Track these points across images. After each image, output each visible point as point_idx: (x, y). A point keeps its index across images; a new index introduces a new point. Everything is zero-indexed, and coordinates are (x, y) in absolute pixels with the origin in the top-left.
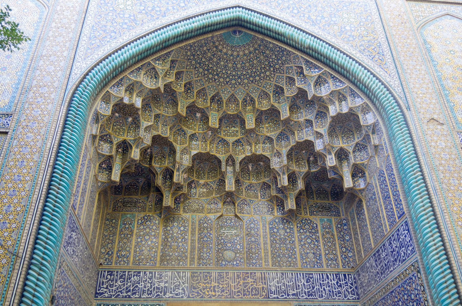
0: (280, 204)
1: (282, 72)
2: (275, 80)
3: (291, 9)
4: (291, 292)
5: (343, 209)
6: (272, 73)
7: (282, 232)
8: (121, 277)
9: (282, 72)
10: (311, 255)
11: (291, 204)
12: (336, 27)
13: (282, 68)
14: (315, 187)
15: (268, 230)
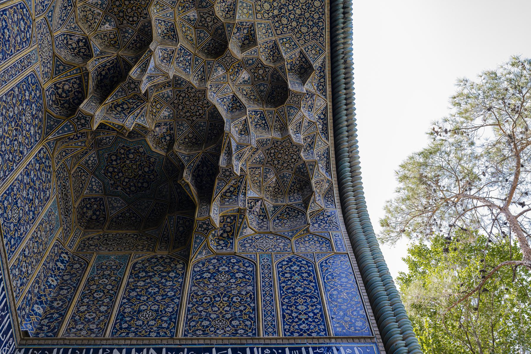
0: (60, 91)
1: (279, 32)
2: (259, 21)
5: (78, 241)
6: (271, 14)
9: (279, 32)
13: (285, 29)
14: (87, 162)
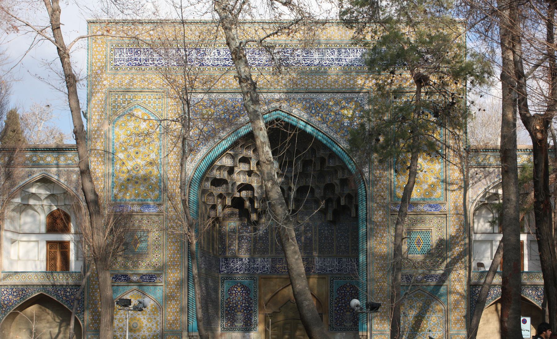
3: (311, 109)
4: (329, 269)
7: (326, 232)
8: (232, 262)
10: (343, 247)
11: (330, 217)
12: (338, 124)
15: (317, 231)
